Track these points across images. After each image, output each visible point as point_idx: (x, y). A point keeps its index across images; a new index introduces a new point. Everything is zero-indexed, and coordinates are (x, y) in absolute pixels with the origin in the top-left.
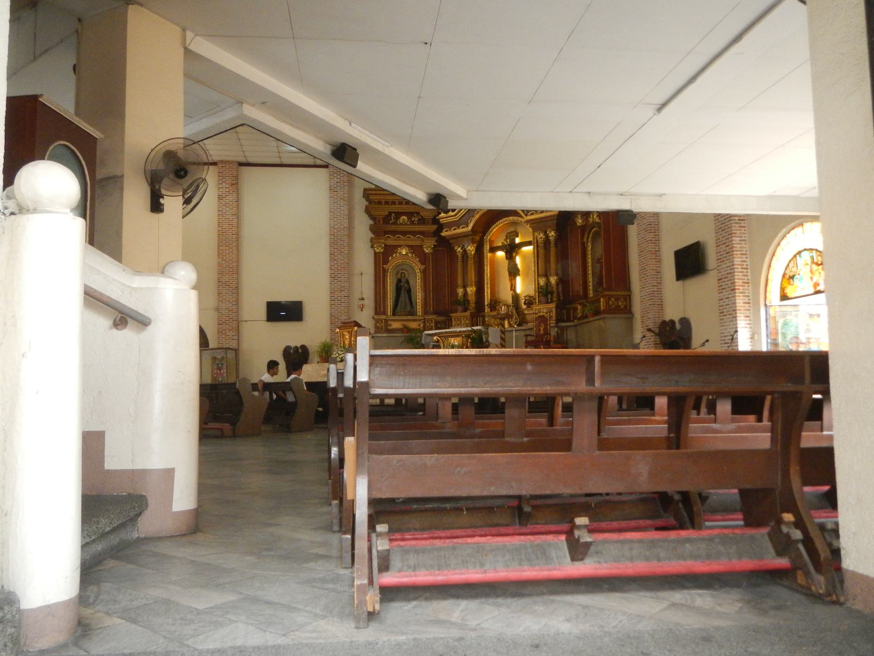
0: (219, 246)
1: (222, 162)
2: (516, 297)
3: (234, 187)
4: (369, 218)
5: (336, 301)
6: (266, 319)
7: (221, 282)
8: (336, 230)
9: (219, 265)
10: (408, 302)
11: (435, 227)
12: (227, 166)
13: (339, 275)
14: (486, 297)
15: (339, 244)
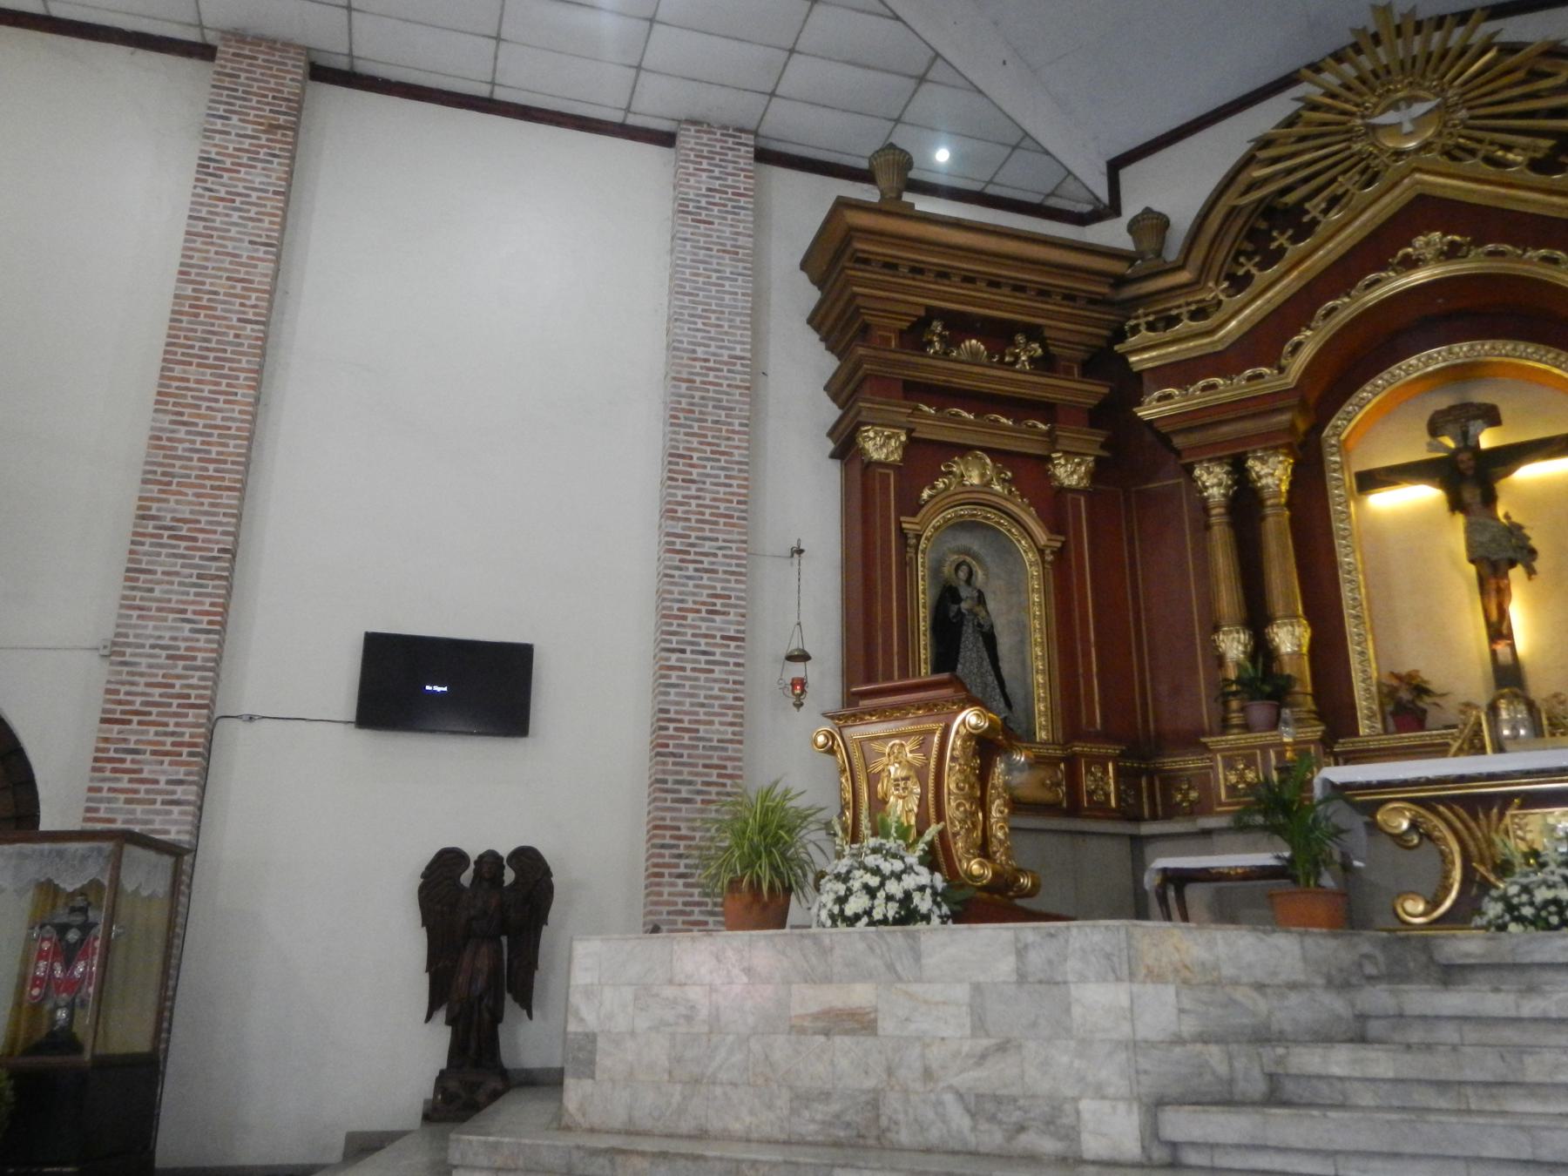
0: (168, 361)
1: (238, 36)
2: (1508, 676)
3: (279, 137)
4: (822, 346)
5: (688, 655)
6: (352, 716)
7: (153, 518)
8: (698, 364)
10: (991, 679)
11: (1092, 391)
12: (262, 56)
13: (708, 543)
14: (1357, 677)
15: (710, 418)
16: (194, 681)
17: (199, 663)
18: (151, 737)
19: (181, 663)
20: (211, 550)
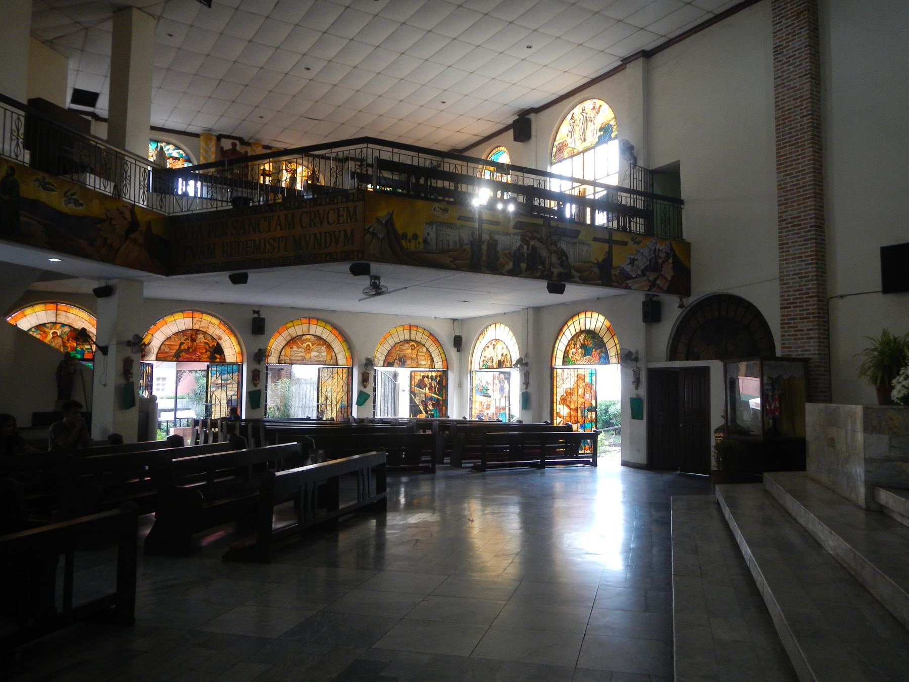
3: (802, 17)
6: (880, 289)
7: (785, 220)
9: (781, 187)
16: (810, 286)
17: (810, 278)
18: (798, 312)
19: (804, 280)
20: (807, 228)
